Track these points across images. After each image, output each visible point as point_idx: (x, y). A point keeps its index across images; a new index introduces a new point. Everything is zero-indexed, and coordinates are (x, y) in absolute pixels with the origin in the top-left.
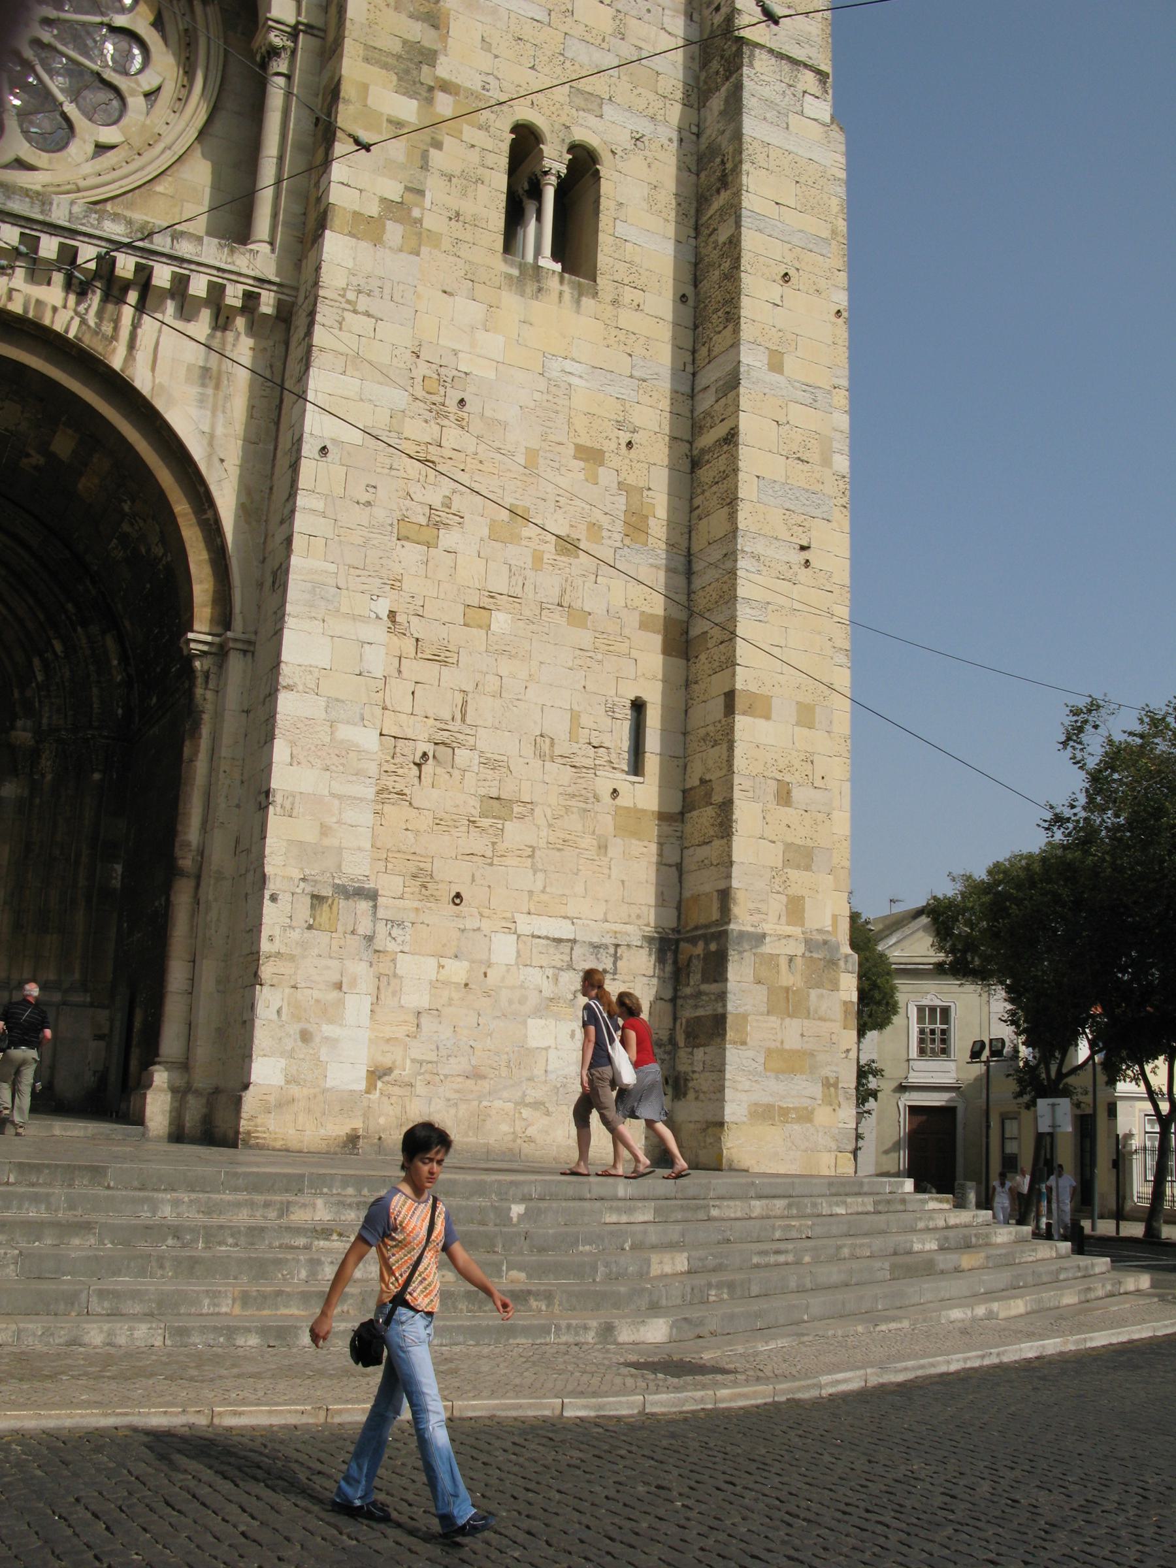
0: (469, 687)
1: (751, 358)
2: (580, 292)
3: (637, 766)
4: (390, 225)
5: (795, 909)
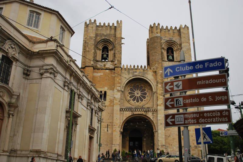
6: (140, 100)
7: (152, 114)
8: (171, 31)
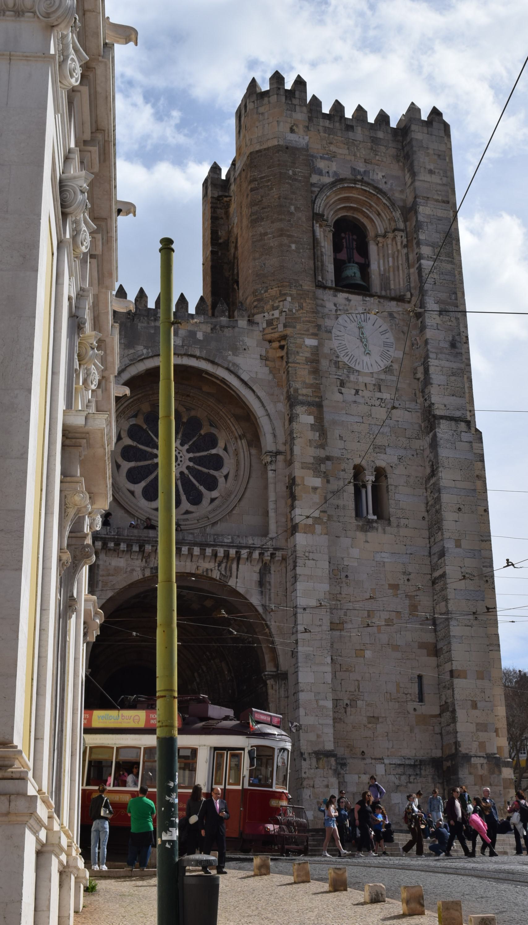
0: (360, 679)
1: (449, 545)
3: (421, 699)
4: (316, 526)
5: (482, 745)
8: (359, 130)
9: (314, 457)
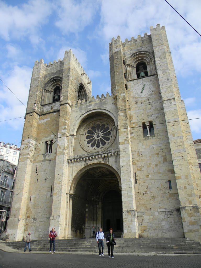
2: (153, 137)
3: (170, 188)
5: (190, 202)
6: (101, 144)
7: (114, 160)
9: (124, 124)
